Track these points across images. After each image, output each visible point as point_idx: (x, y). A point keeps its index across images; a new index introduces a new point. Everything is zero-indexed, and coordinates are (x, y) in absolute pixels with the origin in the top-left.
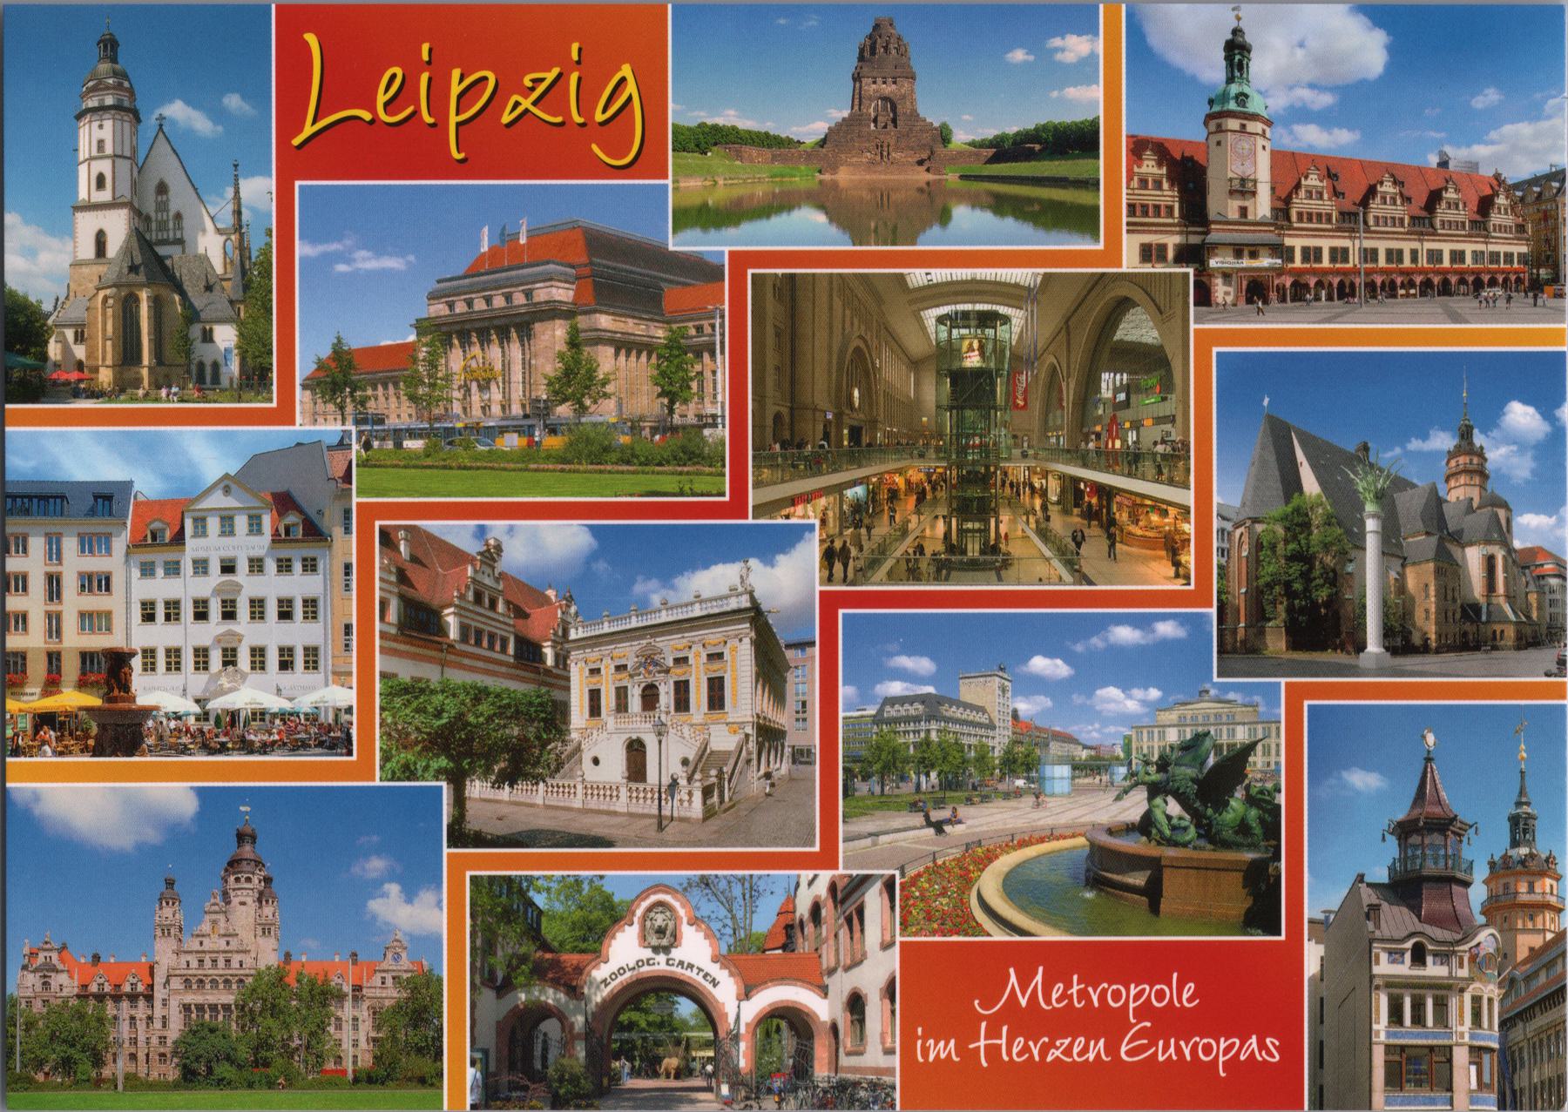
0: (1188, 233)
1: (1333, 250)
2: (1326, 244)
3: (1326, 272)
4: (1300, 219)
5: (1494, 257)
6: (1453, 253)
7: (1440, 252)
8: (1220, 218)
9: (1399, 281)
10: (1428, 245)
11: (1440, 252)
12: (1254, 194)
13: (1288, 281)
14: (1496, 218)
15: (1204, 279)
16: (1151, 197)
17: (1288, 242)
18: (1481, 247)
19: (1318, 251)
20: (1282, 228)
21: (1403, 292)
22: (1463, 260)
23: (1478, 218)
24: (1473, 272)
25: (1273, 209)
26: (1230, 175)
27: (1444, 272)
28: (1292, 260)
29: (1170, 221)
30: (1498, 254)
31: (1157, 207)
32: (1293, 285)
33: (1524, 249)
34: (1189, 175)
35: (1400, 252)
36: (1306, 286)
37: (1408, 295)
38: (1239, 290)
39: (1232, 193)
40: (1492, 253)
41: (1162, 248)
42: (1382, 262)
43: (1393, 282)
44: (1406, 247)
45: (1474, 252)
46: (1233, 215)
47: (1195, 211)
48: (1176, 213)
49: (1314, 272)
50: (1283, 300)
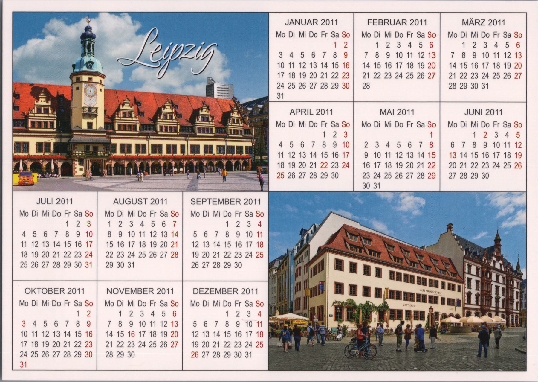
0: (61, 137)
1: (137, 146)
2: (133, 142)
4: (119, 129)
6: (206, 147)
7: (198, 146)
8: (78, 129)
9: (174, 163)
10: (191, 143)
11: (198, 146)
12: (96, 116)
13: (113, 163)
14: (231, 126)
15: (68, 161)
16: (42, 117)
17: (113, 141)
18: (223, 143)
19: (129, 146)
20: (110, 134)
21: (176, 170)
22: (211, 151)
23: (221, 126)
24: (216, 158)
25: (105, 123)
26: (84, 105)
27: (200, 159)
28: (115, 151)
29: (52, 130)
30: (233, 147)
31: (46, 123)
32: (115, 165)
33: (250, 144)
34: (62, 105)
35: (175, 147)
36: (123, 166)
37: (178, 172)
38: (87, 168)
39: (85, 116)
40: (229, 147)
41: (48, 144)
42: (164, 153)
43: (170, 164)
44: (178, 143)
45: (217, 146)
46: (85, 126)
47: (65, 125)
48: (55, 127)
49: (127, 158)
50: (110, 174)
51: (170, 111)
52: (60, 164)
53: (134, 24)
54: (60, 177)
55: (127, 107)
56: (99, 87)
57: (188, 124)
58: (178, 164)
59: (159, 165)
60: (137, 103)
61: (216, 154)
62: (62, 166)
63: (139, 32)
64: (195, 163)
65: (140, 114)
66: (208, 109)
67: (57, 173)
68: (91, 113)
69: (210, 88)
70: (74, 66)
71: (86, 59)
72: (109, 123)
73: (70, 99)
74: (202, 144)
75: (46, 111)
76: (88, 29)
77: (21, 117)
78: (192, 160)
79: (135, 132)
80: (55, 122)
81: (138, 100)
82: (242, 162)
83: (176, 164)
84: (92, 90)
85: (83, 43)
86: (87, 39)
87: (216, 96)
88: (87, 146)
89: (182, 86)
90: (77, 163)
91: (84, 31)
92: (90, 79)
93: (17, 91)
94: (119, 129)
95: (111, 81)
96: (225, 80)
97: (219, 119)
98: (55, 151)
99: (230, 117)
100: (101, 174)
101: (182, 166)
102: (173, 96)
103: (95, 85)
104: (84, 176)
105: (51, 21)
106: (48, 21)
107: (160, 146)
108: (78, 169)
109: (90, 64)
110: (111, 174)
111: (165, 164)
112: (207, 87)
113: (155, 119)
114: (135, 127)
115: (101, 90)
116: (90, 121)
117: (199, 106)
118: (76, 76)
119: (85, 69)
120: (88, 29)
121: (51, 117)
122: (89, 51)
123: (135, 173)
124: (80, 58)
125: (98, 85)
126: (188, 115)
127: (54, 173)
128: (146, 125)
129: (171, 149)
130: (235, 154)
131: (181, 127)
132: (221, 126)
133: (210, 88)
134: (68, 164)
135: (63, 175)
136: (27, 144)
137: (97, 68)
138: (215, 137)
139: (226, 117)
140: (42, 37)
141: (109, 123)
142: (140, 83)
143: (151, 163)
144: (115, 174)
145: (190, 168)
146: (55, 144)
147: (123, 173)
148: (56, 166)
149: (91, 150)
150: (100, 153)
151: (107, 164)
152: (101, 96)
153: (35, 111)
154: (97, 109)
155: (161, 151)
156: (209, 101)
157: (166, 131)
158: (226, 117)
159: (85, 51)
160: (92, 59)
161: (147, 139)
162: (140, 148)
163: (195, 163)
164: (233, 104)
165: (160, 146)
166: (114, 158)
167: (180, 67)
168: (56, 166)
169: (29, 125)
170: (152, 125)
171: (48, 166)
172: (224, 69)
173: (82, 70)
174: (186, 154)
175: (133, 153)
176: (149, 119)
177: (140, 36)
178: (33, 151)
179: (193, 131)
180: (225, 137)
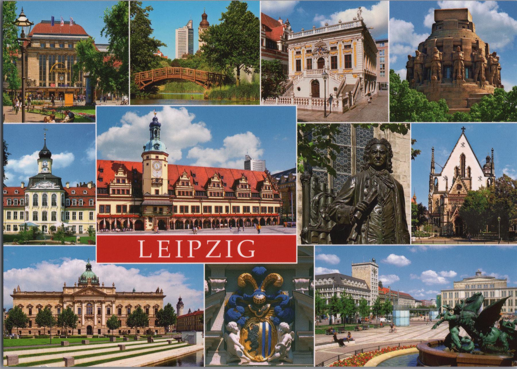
0: (135, 201)
1: (193, 207)
2: (190, 205)
3: (188, 217)
4: (179, 194)
5: (264, 209)
6: (244, 208)
7: (238, 207)
8: (148, 195)
9: (220, 220)
11: (238, 207)
12: (161, 184)
13: (174, 221)
14: (264, 192)
15: (141, 219)
16: (121, 186)
17: (175, 204)
19: (187, 207)
20: (172, 198)
21: (222, 225)
22: (249, 211)
23: (256, 192)
25: (169, 190)
26: (152, 177)
27: (240, 216)
28: (176, 211)
29: (128, 196)
30: (266, 207)
31: (123, 190)
32: (176, 222)
33: (278, 205)
34: (136, 177)
36: (182, 222)
37: (224, 226)
38: (155, 224)
39: (153, 184)
40: (262, 207)
41: (125, 207)
42: (213, 212)
43: (218, 221)
44: (224, 205)
45: (253, 207)
46: (153, 193)
47: (138, 191)
48: (131, 193)
49: (185, 217)
51: (218, 181)
52: (134, 221)
53: (190, 115)
54: (134, 231)
55: (185, 178)
56: (164, 163)
57: (231, 190)
58: (223, 221)
59: (209, 221)
60: (193, 175)
61: (252, 213)
62: (136, 222)
63: (193, 122)
64: (236, 219)
65: (195, 183)
66: (246, 179)
67: (132, 228)
68: (158, 182)
69: (247, 163)
70: (145, 147)
71: (154, 142)
72: (172, 191)
73: (142, 172)
74: (241, 205)
75: (124, 182)
76: (155, 119)
77: (105, 186)
78: (234, 218)
79: (191, 197)
80: (131, 189)
81: (193, 172)
82: (272, 219)
83: (222, 221)
84: (158, 165)
85: (152, 130)
86: (155, 127)
87: (252, 169)
88: (155, 207)
89: (227, 162)
90: (147, 220)
91: (152, 121)
92: (157, 157)
93: (101, 167)
94: (179, 194)
95: (173, 158)
96: (259, 156)
97: (254, 186)
98: (131, 211)
99: (263, 185)
100: (165, 229)
101: (226, 222)
102: (220, 169)
103: (161, 162)
104: (153, 230)
105: (127, 113)
106: (124, 113)
107: (210, 207)
108: (148, 225)
109: (157, 146)
110: (173, 229)
111: (214, 220)
112: (245, 162)
113: (206, 187)
114: (191, 193)
115: (165, 165)
116: (157, 188)
117: (239, 176)
118: (146, 155)
119: (153, 149)
120: (155, 119)
121: (128, 185)
122: (156, 136)
123: (191, 227)
124: (149, 141)
125: (163, 161)
126: (230, 184)
127: (129, 228)
128: (200, 191)
129: (218, 209)
130: (267, 213)
131: (226, 192)
132: (256, 192)
133: (247, 163)
134: (141, 221)
135: (136, 230)
136: (109, 207)
137: (162, 149)
138: (251, 200)
139: (260, 185)
140: (120, 125)
141: (172, 190)
142: (195, 160)
143: (203, 220)
144: (176, 229)
145: (232, 224)
146: (131, 206)
147: (182, 228)
148: (131, 223)
149: (158, 210)
150: (165, 213)
151: (170, 221)
152: (165, 170)
153: (115, 181)
154: (162, 179)
155: (210, 211)
156: (246, 173)
157: (215, 196)
158: (260, 185)
159: (153, 136)
160: (159, 142)
161: (200, 202)
162: (195, 209)
163: (236, 219)
164: (265, 175)
165: (210, 207)
166: (176, 217)
167: (225, 147)
168: (131, 223)
169: (111, 192)
170: (204, 192)
171: (125, 223)
172: (258, 148)
173: (150, 150)
174: (229, 213)
175: (190, 213)
176: (202, 187)
177: (194, 125)
178: (113, 211)
179: (235, 195)
180: (259, 200)
